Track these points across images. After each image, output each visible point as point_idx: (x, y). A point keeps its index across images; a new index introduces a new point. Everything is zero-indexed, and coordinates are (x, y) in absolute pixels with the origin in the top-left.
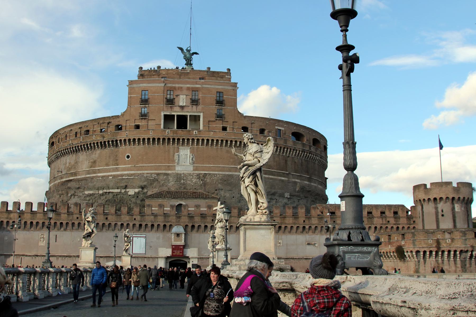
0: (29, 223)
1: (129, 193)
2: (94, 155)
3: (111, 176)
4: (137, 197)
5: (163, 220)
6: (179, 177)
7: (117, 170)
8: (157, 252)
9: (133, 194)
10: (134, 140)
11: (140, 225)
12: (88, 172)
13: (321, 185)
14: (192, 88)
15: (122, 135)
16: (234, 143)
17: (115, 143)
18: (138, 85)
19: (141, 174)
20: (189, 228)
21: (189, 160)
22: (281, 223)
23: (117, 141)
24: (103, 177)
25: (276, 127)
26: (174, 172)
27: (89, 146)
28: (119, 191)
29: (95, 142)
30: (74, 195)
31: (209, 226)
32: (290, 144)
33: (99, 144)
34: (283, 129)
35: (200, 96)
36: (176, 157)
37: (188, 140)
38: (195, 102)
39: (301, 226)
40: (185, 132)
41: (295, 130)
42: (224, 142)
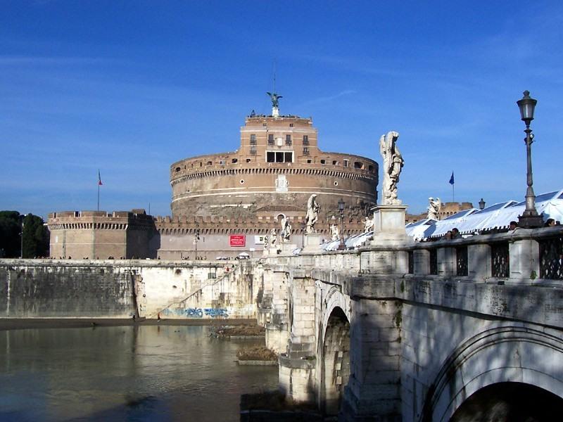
0: (185, 230)
2: (216, 180)
6: (278, 196)
7: (234, 190)
11: (259, 230)
12: (212, 192)
15: (238, 166)
17: (232, 172)
21: (285, 184)
23: (233, 171)
24: (224, 195)
28: (234, 205)
30: (201, 208)
32: (353, 170)
35: (292, 138)
36: (276, 182)
38: (288, 142)
41: (356, 160)
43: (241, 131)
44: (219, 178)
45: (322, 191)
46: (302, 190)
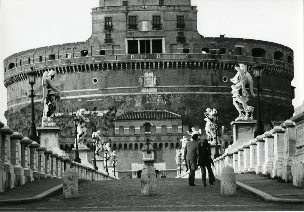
1: (98, 115)
2: (61, 79)
3: (80, 99)
4: (107, 118)
6: (144, 98)
7: (85, 93)
8: (130, 168)
9: (102, 115)
10: (100, 65)
13: (284, 97)
17: (82, 68)
19: (109, 96)
23: (83, 66)
24: (71, 100)
25: (236, 46)
26: (139, 93)
29: (62, 67)
31: (175, 143)
33: (66, 69)
34: (243, 47)
45: (205, 89)
46: (178, 89)
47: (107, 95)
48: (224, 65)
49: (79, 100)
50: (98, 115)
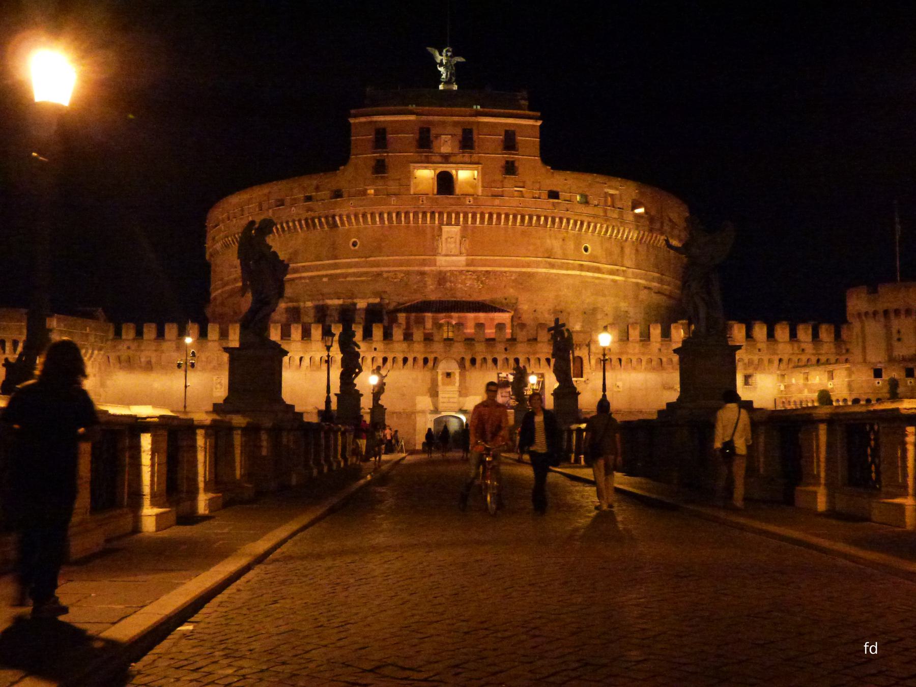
3: (326, 276)
5: (422, 349)
6: (442, 278)
7: (336, 266)
8: (415, 405)
11: (385, 360)
14: (464, 122)
16: (535, 218)
18: (369, 119)
20: (468, 363)
22: (621, 353)
23: (333, 217)
24: (311, 278)
25: (606, 190)
26: (433, 268)
27: (285, 225)
29: (297, 219)
31: (500, 359)
33: (303, 222)
37: (457, 214)
39: (655, 359)
40: (452, 201)
42: (519, 217)
43: (352, 121)
44: (301, 234)
45: (552, 266)
47: (375, 269)
48: (585, 224)
49: (325, 280)
50: (358, 306)
